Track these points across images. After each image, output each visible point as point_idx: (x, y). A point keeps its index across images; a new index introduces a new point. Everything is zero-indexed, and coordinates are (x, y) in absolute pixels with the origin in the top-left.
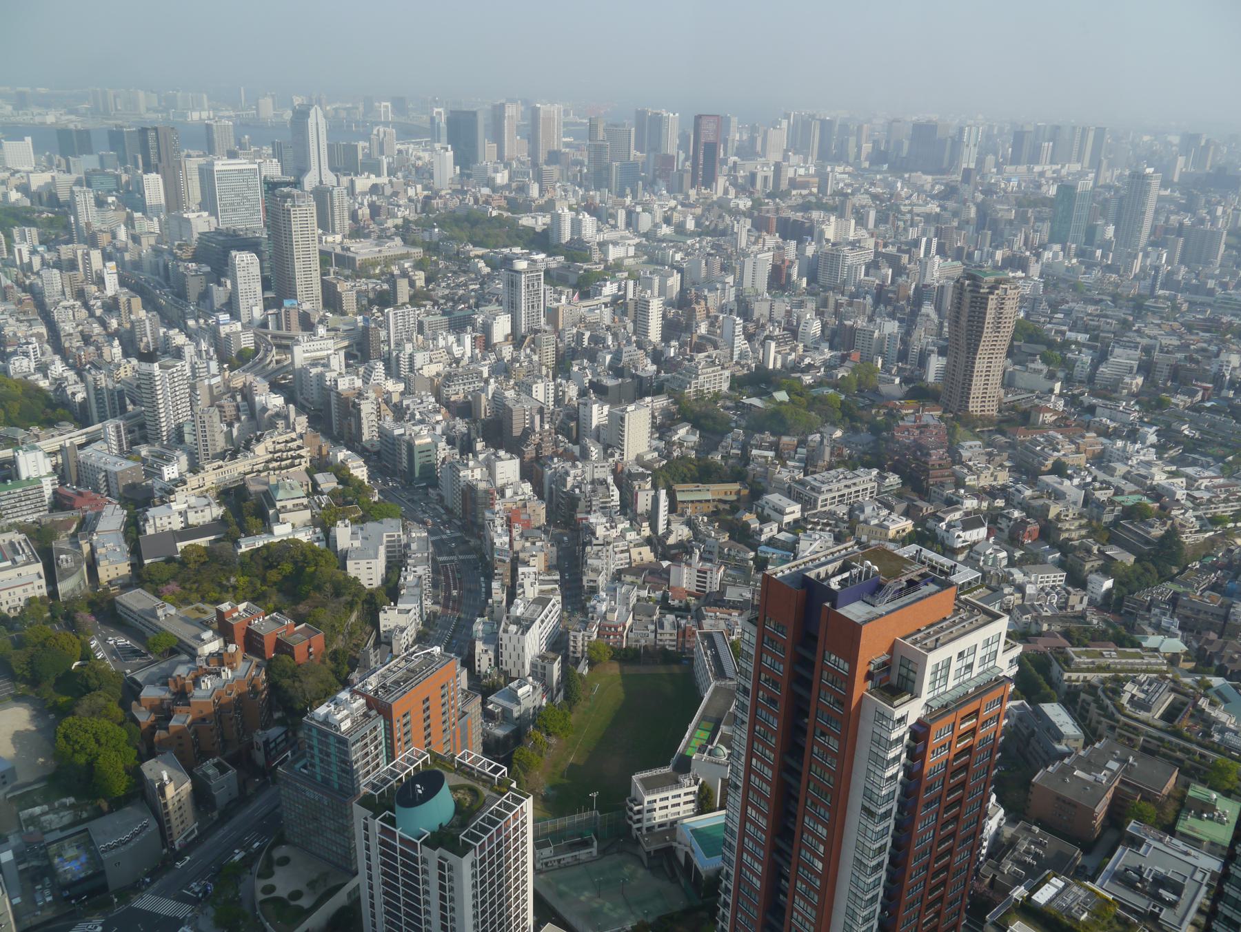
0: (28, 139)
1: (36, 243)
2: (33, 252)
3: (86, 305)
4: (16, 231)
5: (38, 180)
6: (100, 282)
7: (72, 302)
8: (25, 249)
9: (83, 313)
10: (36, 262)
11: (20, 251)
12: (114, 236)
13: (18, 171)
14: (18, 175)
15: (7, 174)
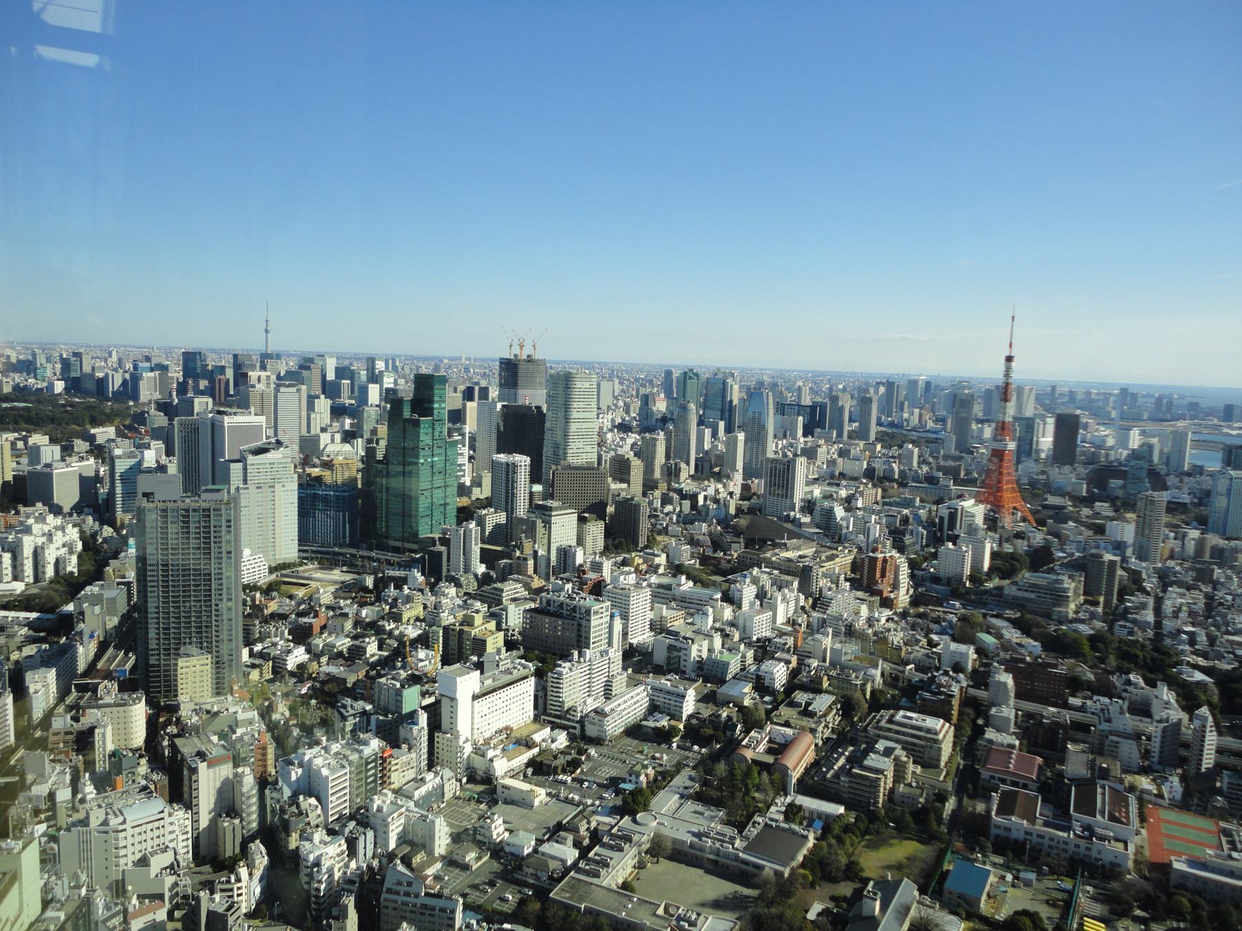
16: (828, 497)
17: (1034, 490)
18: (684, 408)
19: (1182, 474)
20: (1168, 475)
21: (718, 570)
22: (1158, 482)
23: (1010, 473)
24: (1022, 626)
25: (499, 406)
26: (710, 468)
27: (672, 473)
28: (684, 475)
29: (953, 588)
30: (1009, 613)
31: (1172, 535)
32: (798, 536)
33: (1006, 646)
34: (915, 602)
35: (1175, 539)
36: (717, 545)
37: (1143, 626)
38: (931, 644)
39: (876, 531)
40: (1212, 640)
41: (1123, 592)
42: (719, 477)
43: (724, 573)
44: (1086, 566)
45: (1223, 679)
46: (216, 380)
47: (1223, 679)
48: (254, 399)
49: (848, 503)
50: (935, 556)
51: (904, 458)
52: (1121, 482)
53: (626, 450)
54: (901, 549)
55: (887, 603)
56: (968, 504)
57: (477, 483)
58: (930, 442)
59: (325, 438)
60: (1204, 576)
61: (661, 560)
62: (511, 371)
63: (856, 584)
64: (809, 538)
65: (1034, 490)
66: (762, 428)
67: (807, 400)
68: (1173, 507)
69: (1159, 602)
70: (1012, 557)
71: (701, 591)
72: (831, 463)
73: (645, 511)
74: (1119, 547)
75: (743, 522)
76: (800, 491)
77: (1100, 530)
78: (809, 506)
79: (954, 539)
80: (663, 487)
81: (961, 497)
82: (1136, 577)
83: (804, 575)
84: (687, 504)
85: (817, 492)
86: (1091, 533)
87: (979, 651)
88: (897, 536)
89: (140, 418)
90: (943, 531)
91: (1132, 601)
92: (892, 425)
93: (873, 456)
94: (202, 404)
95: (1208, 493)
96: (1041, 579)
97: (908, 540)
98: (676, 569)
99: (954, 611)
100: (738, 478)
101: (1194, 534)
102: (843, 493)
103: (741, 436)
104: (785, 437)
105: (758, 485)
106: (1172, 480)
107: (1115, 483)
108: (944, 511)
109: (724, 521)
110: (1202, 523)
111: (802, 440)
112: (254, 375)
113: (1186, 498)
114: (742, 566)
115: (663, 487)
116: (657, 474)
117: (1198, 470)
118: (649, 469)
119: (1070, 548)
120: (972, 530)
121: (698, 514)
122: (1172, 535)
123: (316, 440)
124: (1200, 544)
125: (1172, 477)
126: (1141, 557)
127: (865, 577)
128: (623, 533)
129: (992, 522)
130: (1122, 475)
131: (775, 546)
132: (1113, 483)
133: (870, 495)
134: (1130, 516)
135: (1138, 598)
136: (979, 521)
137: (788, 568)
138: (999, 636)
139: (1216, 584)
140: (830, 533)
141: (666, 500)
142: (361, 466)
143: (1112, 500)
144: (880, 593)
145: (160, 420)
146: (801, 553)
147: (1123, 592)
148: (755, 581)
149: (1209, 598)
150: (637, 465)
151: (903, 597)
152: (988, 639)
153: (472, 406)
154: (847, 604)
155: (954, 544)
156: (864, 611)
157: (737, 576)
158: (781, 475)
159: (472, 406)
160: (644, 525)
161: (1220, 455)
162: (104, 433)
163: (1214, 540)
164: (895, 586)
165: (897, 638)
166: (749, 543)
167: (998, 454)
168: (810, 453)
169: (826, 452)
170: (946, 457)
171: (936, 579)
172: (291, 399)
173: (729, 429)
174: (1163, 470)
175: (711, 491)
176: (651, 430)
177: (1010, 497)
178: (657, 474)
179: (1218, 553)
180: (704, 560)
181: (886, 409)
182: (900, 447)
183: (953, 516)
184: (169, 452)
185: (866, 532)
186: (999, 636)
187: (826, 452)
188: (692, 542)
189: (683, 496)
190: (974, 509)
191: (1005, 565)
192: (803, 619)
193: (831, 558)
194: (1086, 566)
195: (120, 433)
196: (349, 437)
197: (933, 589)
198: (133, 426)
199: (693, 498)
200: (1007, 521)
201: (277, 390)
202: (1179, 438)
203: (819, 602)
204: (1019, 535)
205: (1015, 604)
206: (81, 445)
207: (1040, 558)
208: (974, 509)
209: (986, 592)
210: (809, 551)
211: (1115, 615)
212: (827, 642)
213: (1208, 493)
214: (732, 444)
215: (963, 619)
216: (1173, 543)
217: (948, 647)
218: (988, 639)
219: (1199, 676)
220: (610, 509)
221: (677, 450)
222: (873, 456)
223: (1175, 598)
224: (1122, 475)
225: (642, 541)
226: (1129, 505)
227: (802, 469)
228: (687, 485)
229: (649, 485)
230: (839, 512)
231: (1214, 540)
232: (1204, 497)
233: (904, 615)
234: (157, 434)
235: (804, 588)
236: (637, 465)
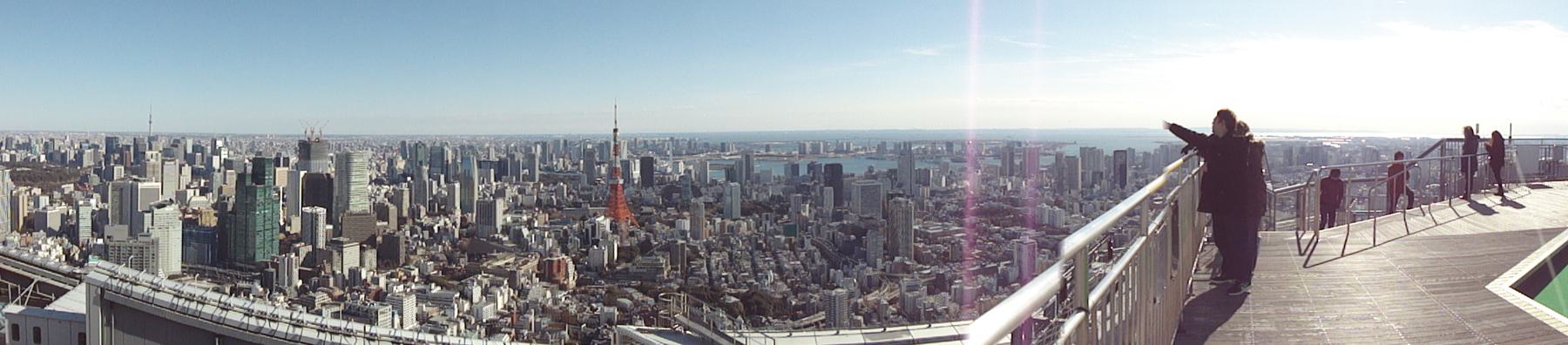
16: (515, 221)
17: (636, 204)
18: (420, 170)
19: (707, 186)
21: (454, 277)
22: (697, 193)
23: (621, 195)
24: (640, 289)
25: (302, 173)
26: (441, 207)
27: (414, 213)
28: (423, 213)
29: (600, 273)
30: (634, 283)
32: (503, 250)
33: (636, 304)
34: (578, 284)
36: (450, 260)
37: (703, 277)
38: (593, 310)
39: (550, 243)
40: (735, 277)
41: (689, 260)
42: (446, 213)
43: (459, 279)
44: (669, 248)
45: (744, 298)
46: (127, 155)
47: (744, 298)
48: (149, 169)
49: (529, 224)
50: (587, 253)
51: (558, 192)
53: (381, 198)
54: (565, 251)
55: (563, 287)
56: (600, 219)
57: (288, 222)
58: (572, 179)
59: (190, 192)
60: (726, 243)
61: (415, 272)
62: (306, 149)
63: (541, 277)
64: (510, 251)
65: (636, 204)
66: (472, 179)
67: (493, 157)
68: (708, 205)
69: (708, 261)
70: (630, 248)
71: (445, 292)
72: (515, 199)
73: (402, 240)
74: (683, 233)
75: (465, 242)
76: (502, 218)
77: (672, 225)
78: (506, 230)
79: (596, 242)
80: (410, 222)
82: (695, 250)
83: (512, 278)
84: (426, 233)
85: (509, 219)
87: (622, 309)
88: (563, 242)
89: (85, 178)
90: (589, 238)
91: (695, 263)
92: (548, 169)
93: (539, 192)
94: (119, 171)
95: (721, 195)
96: (647, 260)
97: (570, 246)
98: (427, 280)
99: (603, 287)
100: (458, 213)
101: (718, 220)
102: (525, 218)
103: (457, 185)
105: (472, 217)
106: (703, 190)
107: (675, 195)
108: (589, 226)
109: (453, 243)
110: (721, 211)
112: (149, 153)
114: (471, 272)
115: (410, 222)
116: (405, 213)
117: (714, 182)
118: (400, 210)
119: (659, 238)
120: (605, 236)
121: (435, 238)
123: (185, 194)
124: (722, 225)
126: (696, 236)
127: (547, 273)
128: (388, 255)
129: (614, 228)
130: (679, 190)
131: (488, 258)
132: (676, 195)
133: (541, 220)
134: (686, 213)
135: (699, 262)
136: (608, 228)
137: (499, 272)
138: (631, 298)
139: (732, 246)
140: (521, 246)
141: (413, 231)
142: (213, 212)
143: (675, 205)
144: (557, 282)
145: (95, 180)
147: (689, 260)
148: (480, 283)
149: (730, 254)
150: (393, 208)
151: (572, 282)
152: (627, 302)
153: (282, 172)
154: (539, 292)
156: (549, 294)
157: (468, 280)
158: (487, 211)
159: (282, 172)
160: (402, 250)
162: (69, 188)
163: (728, 222)
164: (567, 276)
165: (573, 309)
166: (470, 258)
167: (614, 187)
168: (500, 193)
169: (511, 191)
171: (588, 269)
172: (171, 167)
173: (446, 181)
174: (697, 184)
175: (441, 223)
176: (396, 182)
177: (623, 212)
178: (405, 213)
179: (731, 229)
180: (444, 271)
181: (543, 160)
183: (594, 228)
184: (104, 200)
185: (543, 243)
186: (631, 298)
187: (511, 191)
188: (433, 258)
189: (424, 228)
190: (604, 222)
191: (626, 254)
192: (513, 305)
193: (525, 263)
194: (669, 248)
195: (76, 188)
196: (204, 192)
197: (590, 274)
198: (81, 183)
199: (431, 228)
200: (623, 226)
201: (163, 162)
202: (703, 165)
203: (522, 292)
204: (632, 234)
205: (636, 276)
206: (57, 195)
207: (645, 247)
208: (604, 222)
209: (619, 272)
210: (511, 260)
211: (688, 274)
212: (532, 318)
213: (721, 195)
214: (451, 191)
215: (609, 291)
216: (710, 227)
217: (599, 307)
218: (627, 302)
219: (734, 299)
220: (379, 239)
221: (419, 194)
222: (539, 192)
223: (715, 258)
224: (679, 190)
225: (402, 261)
226: (686, 207)
227: (501, 205)
228: (426, 220)
229: (401, 221)
230: (525, 232)
231: (728, 222)
232: (720, 197)
233: (574, 293)
234: (96, 190)
235: (512, 284)
236: (393, 208)
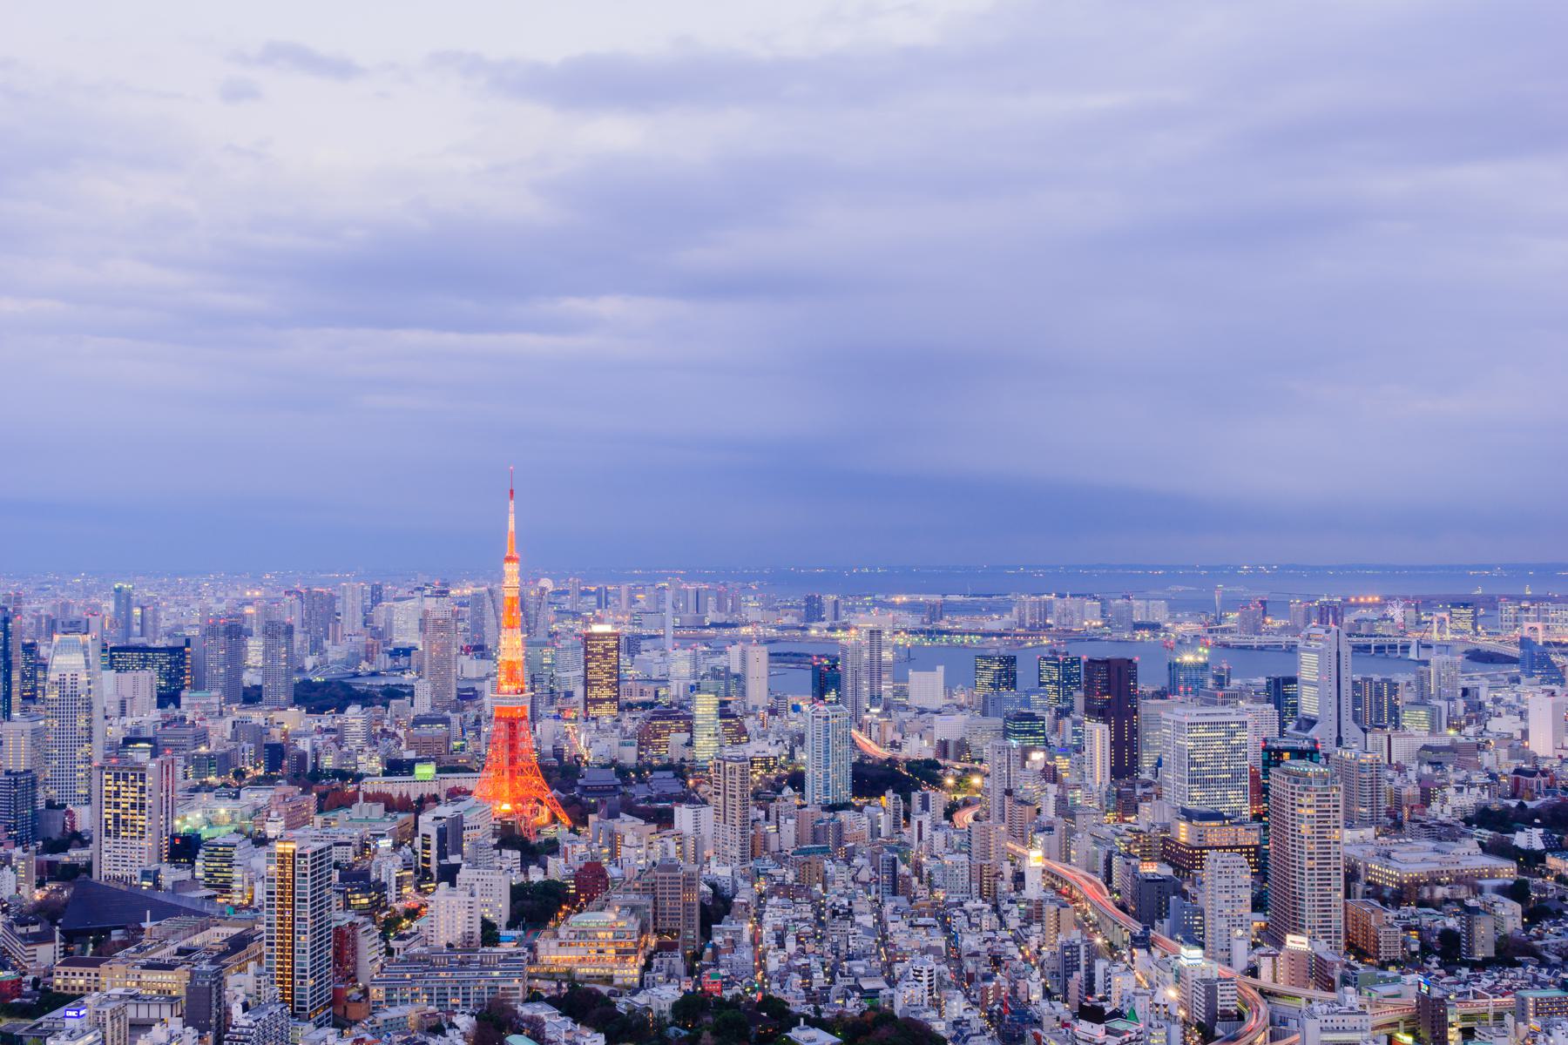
0: (941, 669)
1: (941, 811)
2: (936, 827)
3: (996, 908)
4: (916, 797)
5: (949, 728)
6: (1019, 878)
7: (980, 903)
8: (926, 820)
9: (989, 921)
10: (939, 837)
11: (920, 824)
12: (1039, 811)
13: (922, 711)
14: (923, 717)
15: (911, 714)
20: (747, 714)
31: (762, 813)
35: (767, 818)
52: (685, 737)
78: (184, 848)
79: (449, 874)
81: (455, 794)
86: (653, 827)
104: (123, 713)
111: (155, 714)
113: (773, 751)
122: (762, 813)
125: (752, 718)
146: (183, 944)
155: (453, 884)
161: (807, 676)
166: (69, 937)
170: (418, 721)
182: (341, 710)
